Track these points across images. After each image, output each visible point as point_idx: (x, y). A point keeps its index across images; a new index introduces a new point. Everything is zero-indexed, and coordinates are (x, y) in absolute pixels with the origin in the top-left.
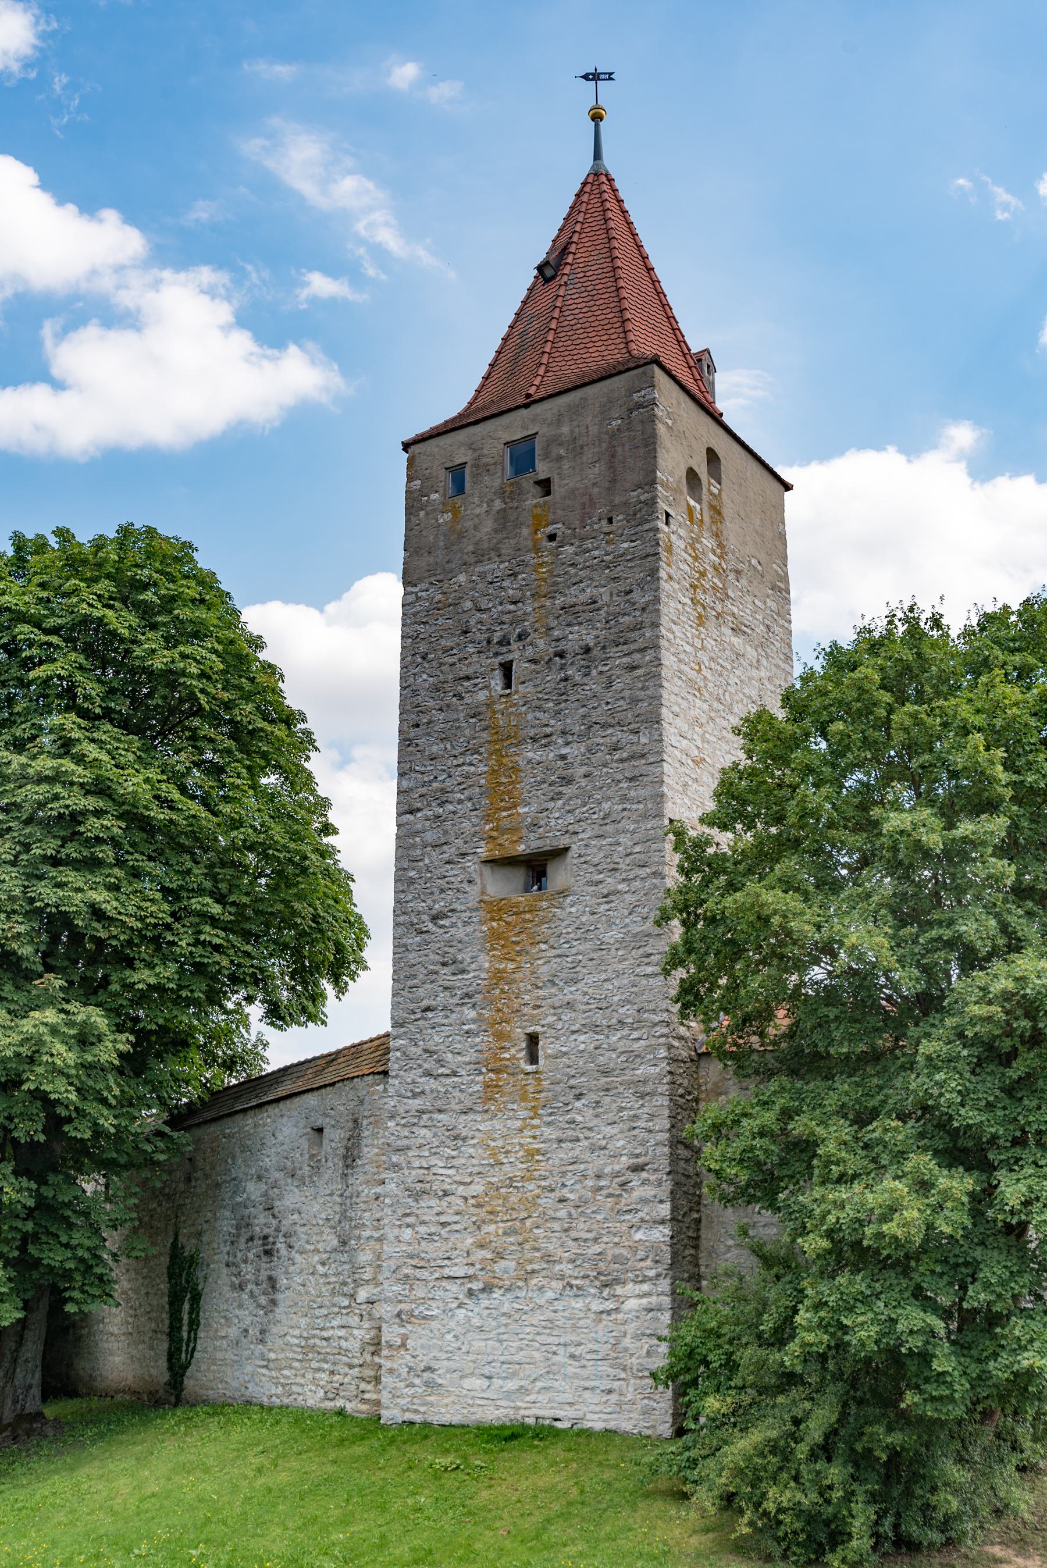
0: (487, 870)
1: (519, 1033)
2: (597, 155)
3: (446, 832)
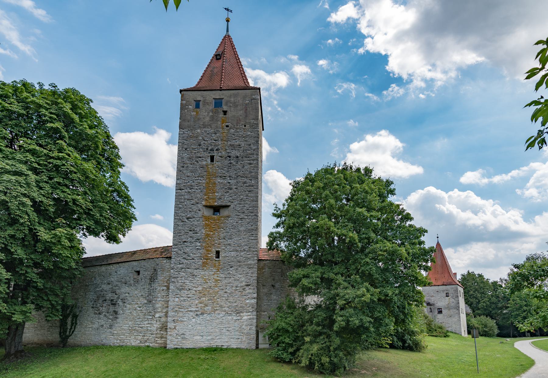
0: (204, 208)
2: (227, 31)
3: (192, 196)
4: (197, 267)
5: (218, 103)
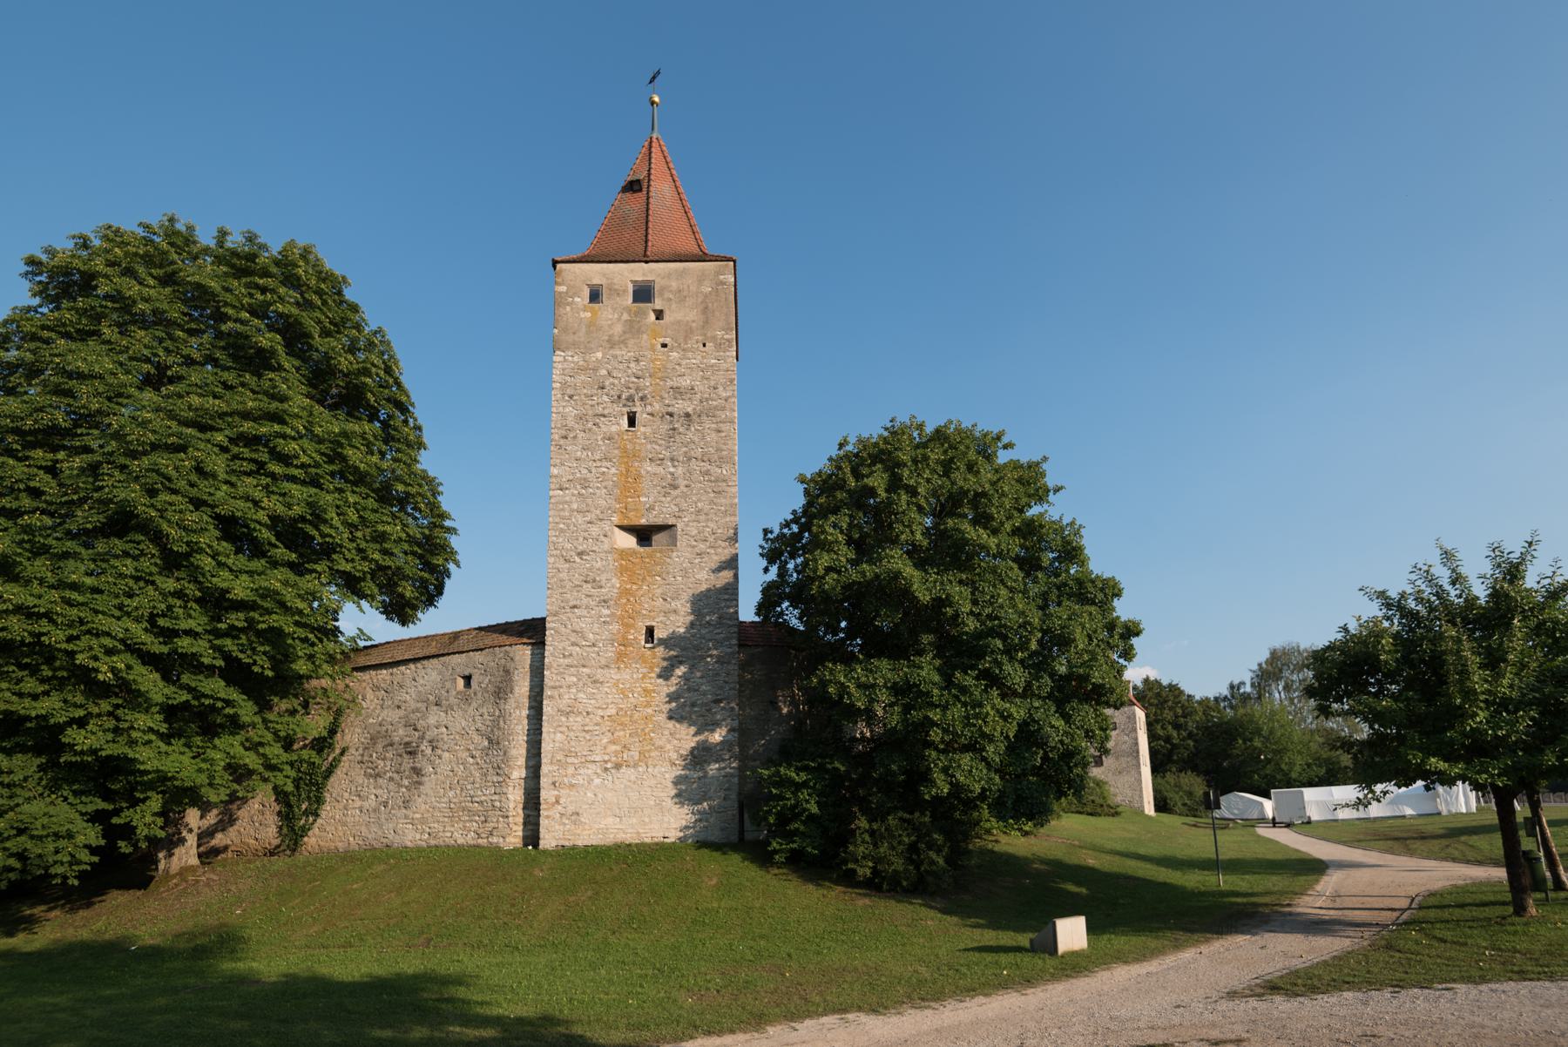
1: (641, 627)
4: (603, 662)
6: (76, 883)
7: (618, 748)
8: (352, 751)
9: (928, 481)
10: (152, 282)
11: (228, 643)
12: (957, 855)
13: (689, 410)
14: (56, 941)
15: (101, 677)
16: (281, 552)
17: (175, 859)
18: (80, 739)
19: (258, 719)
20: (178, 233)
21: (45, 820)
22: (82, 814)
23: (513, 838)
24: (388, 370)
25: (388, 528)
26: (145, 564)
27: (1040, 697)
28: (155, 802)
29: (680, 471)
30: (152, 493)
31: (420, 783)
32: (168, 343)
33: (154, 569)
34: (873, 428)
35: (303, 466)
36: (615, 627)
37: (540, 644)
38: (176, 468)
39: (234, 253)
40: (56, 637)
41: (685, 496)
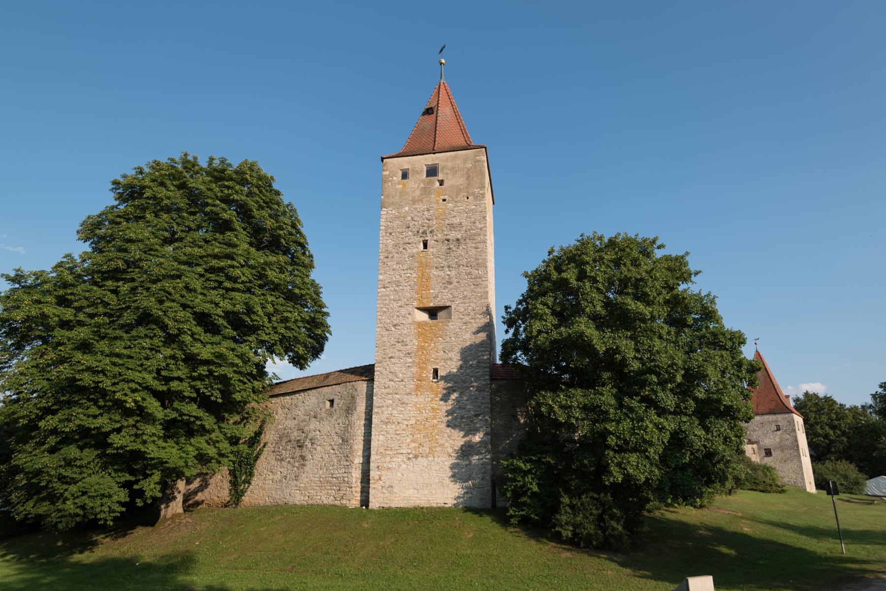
4: (408, 391)
5: (432, 171)
6: (111, 523)
7: (416, 445)
8: (269, 445)
9: (605, 272)
10: (172, 188)
11: (198, 384)
12: (633, 523)
13: (459, 237)
14: (101, 557)
15: (128, 405)
16: (229, 331)
17: (170, 509)
18: (116, 440)
19: (215, 427)
20: (188, 162)
21: (96, 487)
22: (118, 483)
23: (354, 502)
24: (294, 226)
25: (289, 315)
26: (156, 341)
27: (686, 415)
28: (157, 476)
29: (453, 273)
30: (161, 302)
31: (304, 465)
32: (179, 220)
33: (160, 344)
34: (568, 241)
35: (243, 282)
36: (414, 370)
37: (371, 380)
38: (174, 288)
39: (215, 170)
40: (106, 383)
41: (456, 288)
